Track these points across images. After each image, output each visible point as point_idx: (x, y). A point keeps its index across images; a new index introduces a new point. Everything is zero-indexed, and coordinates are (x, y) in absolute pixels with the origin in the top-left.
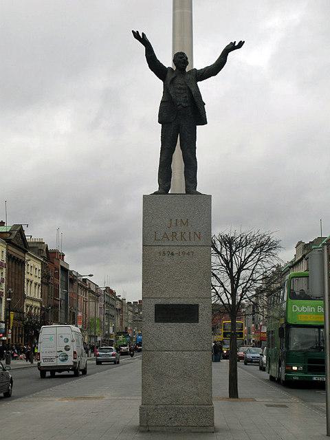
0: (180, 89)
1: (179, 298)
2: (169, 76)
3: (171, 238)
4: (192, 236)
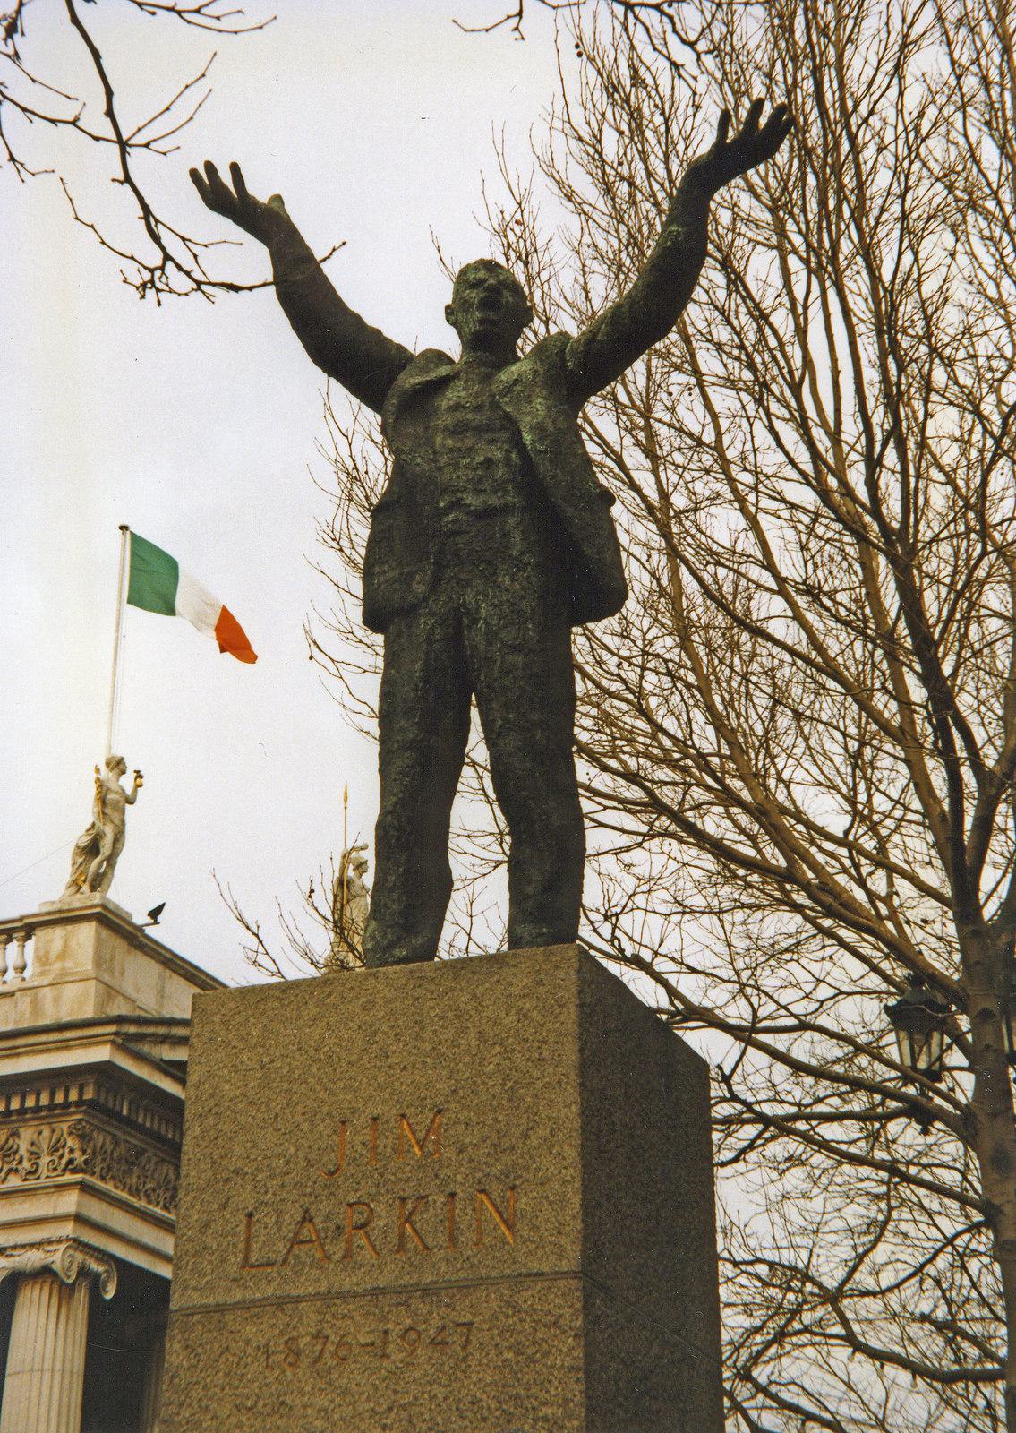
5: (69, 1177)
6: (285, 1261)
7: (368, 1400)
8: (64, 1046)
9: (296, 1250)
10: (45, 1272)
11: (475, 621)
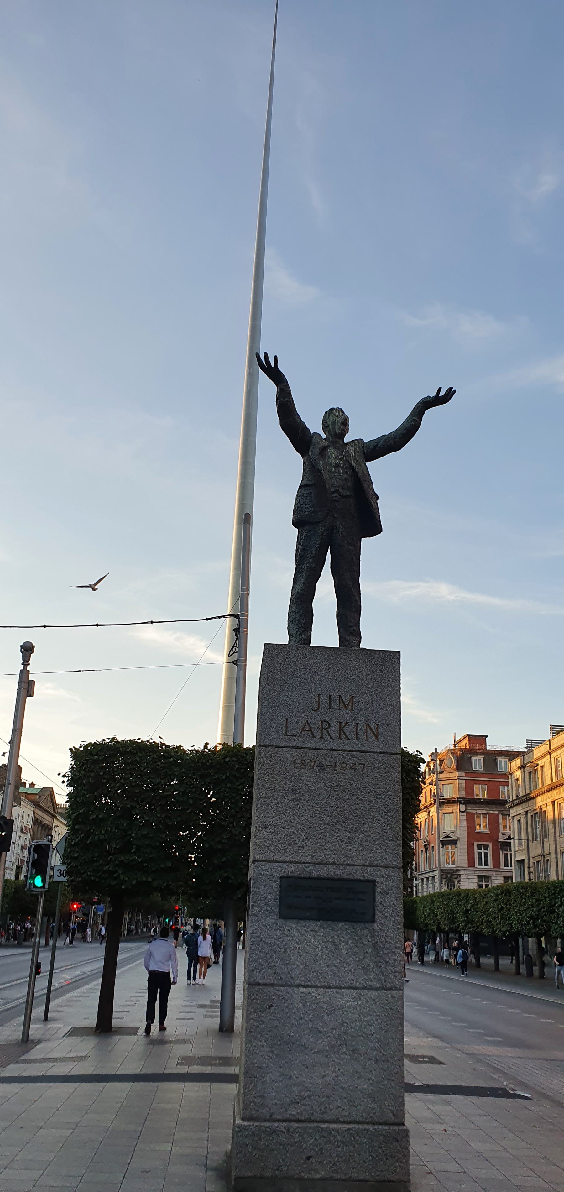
1: (333, 864)
2: (314, 451)
3: (318, 734)
6: (300, 736)
7: (330, 782)
9: (303, 732)
11: (338, 532)
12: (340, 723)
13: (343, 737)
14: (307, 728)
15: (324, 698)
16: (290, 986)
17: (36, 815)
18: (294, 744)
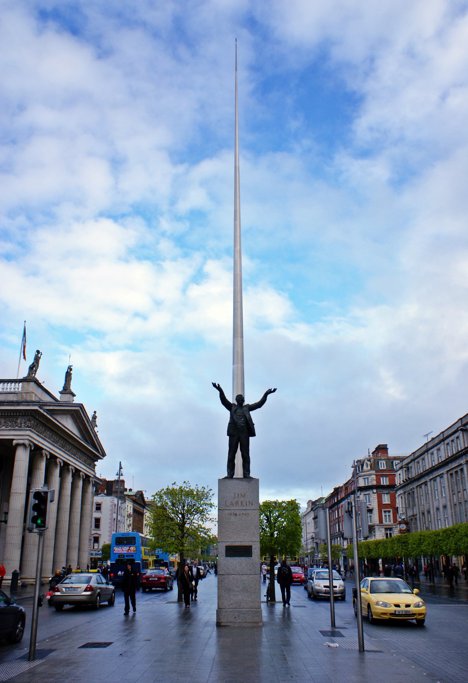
0: (240, 416)
1: (240, 542)
2: (234, 409)
4: (248, 503)
5: (27, 428)
8: (28, 405)
10: (24, 445)
12: (241, 502)
13: (242, 506)
14: (232, 504)
15: (237, 495)
16: (229, 575)
17: (134, 507)
18: (228, 509)
